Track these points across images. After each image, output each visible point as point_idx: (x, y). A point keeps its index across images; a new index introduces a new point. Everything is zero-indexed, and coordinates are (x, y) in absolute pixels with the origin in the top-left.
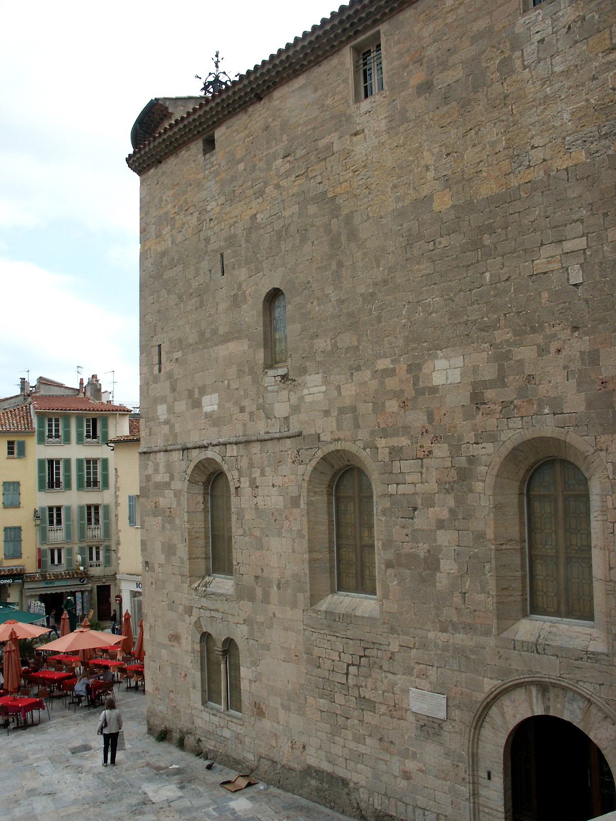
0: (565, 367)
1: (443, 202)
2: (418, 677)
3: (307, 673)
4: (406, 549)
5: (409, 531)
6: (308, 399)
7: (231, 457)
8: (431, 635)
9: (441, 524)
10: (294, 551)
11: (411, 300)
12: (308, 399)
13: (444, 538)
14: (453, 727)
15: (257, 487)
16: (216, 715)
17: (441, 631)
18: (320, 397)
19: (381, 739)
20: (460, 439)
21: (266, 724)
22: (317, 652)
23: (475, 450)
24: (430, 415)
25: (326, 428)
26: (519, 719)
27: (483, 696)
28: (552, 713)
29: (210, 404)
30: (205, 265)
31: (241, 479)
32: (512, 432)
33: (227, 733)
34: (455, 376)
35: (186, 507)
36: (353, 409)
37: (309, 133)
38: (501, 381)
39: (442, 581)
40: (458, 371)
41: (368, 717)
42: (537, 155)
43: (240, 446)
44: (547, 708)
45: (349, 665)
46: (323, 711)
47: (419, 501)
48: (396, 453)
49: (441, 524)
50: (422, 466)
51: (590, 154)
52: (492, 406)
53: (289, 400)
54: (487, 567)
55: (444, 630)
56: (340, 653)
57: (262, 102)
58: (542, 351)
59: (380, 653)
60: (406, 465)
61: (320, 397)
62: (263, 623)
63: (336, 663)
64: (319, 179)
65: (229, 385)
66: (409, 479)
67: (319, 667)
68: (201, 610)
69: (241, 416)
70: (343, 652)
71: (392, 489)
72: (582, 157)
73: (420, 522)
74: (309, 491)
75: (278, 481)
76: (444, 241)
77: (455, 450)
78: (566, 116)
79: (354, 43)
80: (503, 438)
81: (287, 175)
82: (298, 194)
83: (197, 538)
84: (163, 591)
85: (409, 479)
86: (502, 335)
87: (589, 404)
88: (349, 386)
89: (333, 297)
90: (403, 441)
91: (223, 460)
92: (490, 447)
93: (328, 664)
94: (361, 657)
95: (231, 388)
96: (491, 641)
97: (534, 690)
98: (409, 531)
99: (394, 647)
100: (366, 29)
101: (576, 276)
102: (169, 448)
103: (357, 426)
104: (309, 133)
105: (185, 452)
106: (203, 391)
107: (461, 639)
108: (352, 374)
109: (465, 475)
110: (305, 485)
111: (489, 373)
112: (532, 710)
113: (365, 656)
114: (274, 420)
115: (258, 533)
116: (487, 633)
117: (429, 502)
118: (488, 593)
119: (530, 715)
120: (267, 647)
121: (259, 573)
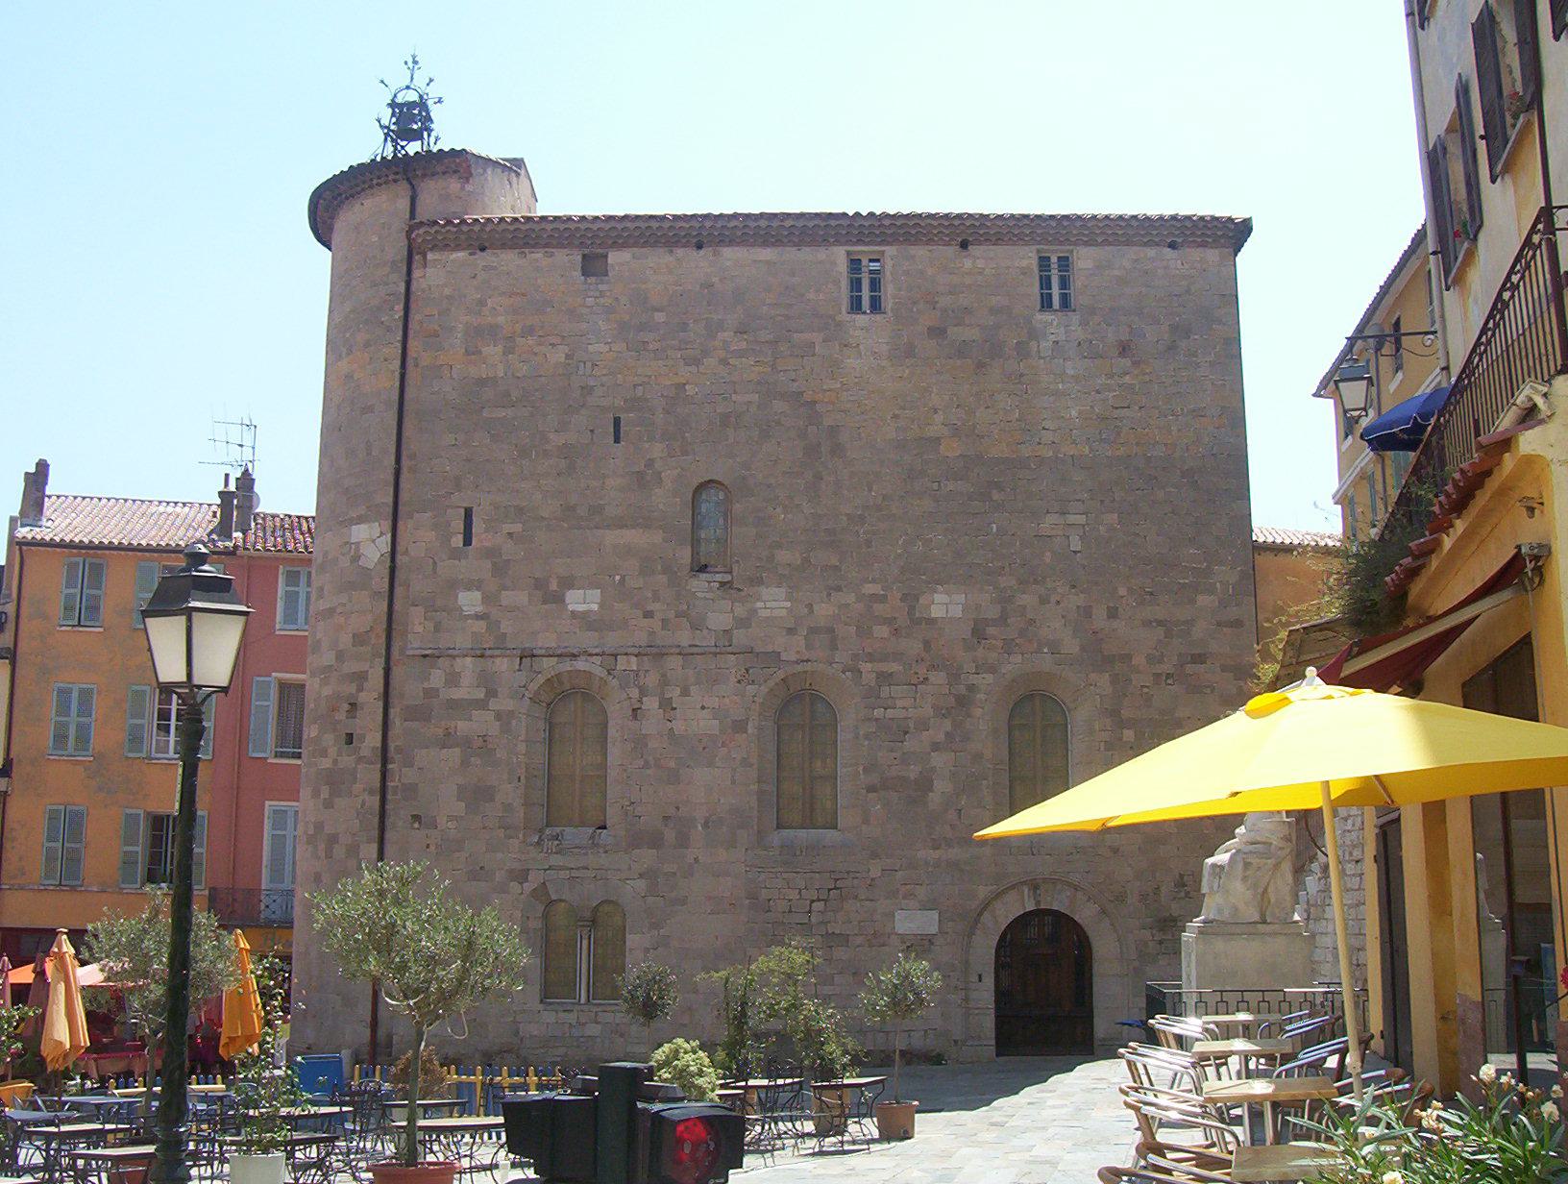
1: (951, 449)
2: (904, 898)
5: (898, 755)
6: (764, 613)
8: (921, 854)
9: (936, 747)
10: (733, 782)
11: (909, 532)
13: (938, 760)
14: (946, 940)
18: (784, 612)
22: (764, 894)
23: (974, 679)
24: (927, 644)
25: (792, 648)
29: (582, 601)
31: (644, 699)
32: (1010, 667)
33: (593, 1030)
34: (957, 611)
35: (524, 732)
36: (831, 630)
38: (1003, 620)
39: (935, 799)
41: (841, 953)
42: (1047, 437)
43: (646, 658)
44: (1038, 903)
47: (912, 725)
49: (936, 747)
50: (916, 692)
51: (1091, 450)
53: (732, 611)
55: (935, 848)
57: (702, 252)
58: (1044, 601)
61: (784, 612)
62: (675, 874)
64: (793, 375)
68: (548, 872)
71: (878, 713)
72: (1087, 450)
73: (910, 744)
75: (714, 702)
77: (954, 676)
78: (1074, 413)
80: (1003, 671)
81: (740, 354)
82: (759, 383)
84: (457, 854)
86: (1005, 581)
87: (1083, 649)
90: (894, 667)
91: (609, 674)
92: (989, 678)
94: (830, 890)
98: (898, 755)
99: (875, 871)
100: (880, 244)
101: (1076, 544)
102: (488, 653)
103: (834, 647)
106: (568, 583)
109: (963, 702)
111: (993, 612)
114: (705, 631)
115: (672, 764)
117: (923, 725)
120: (683, 901)
121: (672, 811)
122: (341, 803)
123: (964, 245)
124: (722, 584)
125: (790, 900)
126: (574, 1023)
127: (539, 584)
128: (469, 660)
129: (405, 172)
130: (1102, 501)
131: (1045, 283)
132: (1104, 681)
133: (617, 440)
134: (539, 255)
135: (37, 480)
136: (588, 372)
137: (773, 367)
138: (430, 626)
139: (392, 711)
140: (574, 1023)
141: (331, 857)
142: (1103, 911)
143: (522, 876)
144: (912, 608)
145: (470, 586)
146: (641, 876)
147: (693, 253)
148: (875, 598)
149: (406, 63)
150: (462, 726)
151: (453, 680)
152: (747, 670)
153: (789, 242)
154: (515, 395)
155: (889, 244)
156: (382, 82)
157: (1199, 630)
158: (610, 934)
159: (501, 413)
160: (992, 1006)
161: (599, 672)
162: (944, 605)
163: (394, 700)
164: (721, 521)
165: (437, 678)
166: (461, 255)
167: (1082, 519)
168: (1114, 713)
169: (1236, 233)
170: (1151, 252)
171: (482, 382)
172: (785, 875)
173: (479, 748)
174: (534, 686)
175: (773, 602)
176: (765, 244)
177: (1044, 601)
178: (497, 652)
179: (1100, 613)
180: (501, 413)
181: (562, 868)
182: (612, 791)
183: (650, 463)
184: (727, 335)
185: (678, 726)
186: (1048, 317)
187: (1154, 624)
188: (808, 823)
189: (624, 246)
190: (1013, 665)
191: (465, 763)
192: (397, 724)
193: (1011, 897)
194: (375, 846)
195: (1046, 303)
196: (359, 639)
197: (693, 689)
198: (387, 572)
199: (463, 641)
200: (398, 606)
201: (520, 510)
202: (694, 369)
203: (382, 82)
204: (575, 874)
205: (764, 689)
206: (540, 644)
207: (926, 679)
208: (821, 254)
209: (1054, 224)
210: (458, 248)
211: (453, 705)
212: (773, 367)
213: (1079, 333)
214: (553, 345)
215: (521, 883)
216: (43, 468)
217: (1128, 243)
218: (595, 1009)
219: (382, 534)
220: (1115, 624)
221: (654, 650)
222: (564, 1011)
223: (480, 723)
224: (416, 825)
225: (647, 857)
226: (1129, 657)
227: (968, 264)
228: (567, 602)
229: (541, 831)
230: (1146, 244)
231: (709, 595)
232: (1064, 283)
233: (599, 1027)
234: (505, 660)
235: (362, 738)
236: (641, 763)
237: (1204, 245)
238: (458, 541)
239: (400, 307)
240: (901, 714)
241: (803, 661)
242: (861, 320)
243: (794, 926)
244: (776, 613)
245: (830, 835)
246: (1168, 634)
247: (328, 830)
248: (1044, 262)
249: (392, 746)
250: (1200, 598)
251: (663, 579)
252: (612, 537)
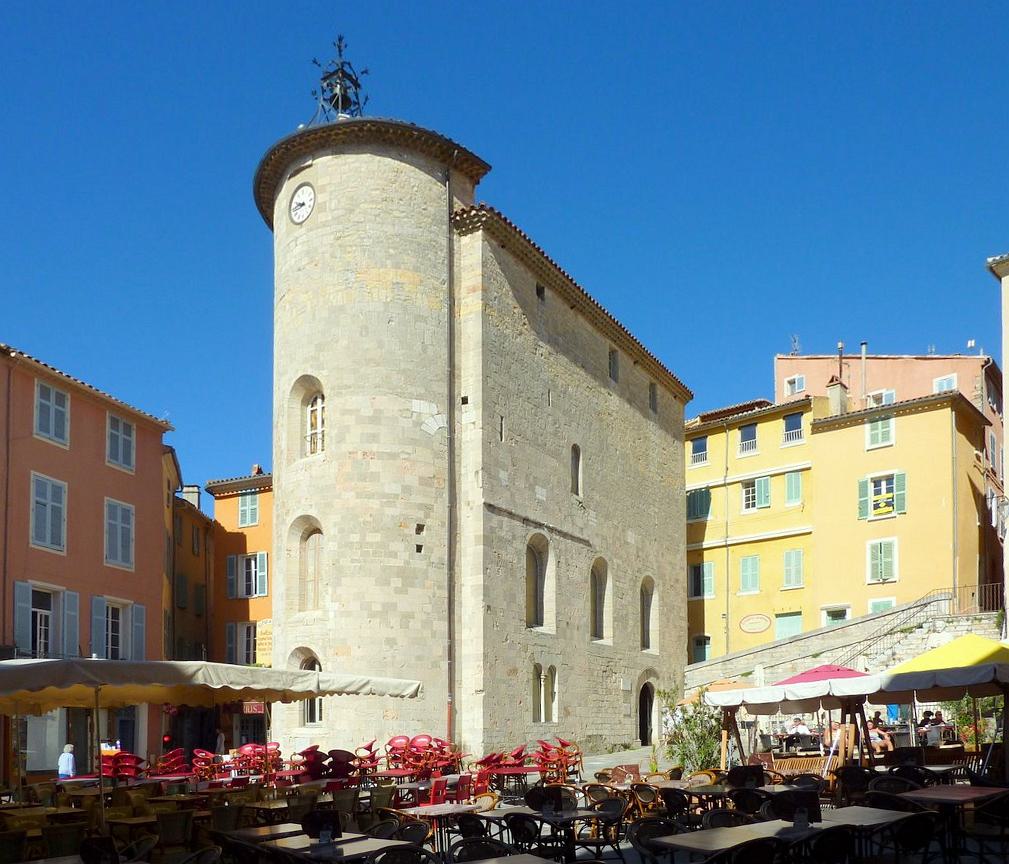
194: (446, 623)
196: (425, 482)
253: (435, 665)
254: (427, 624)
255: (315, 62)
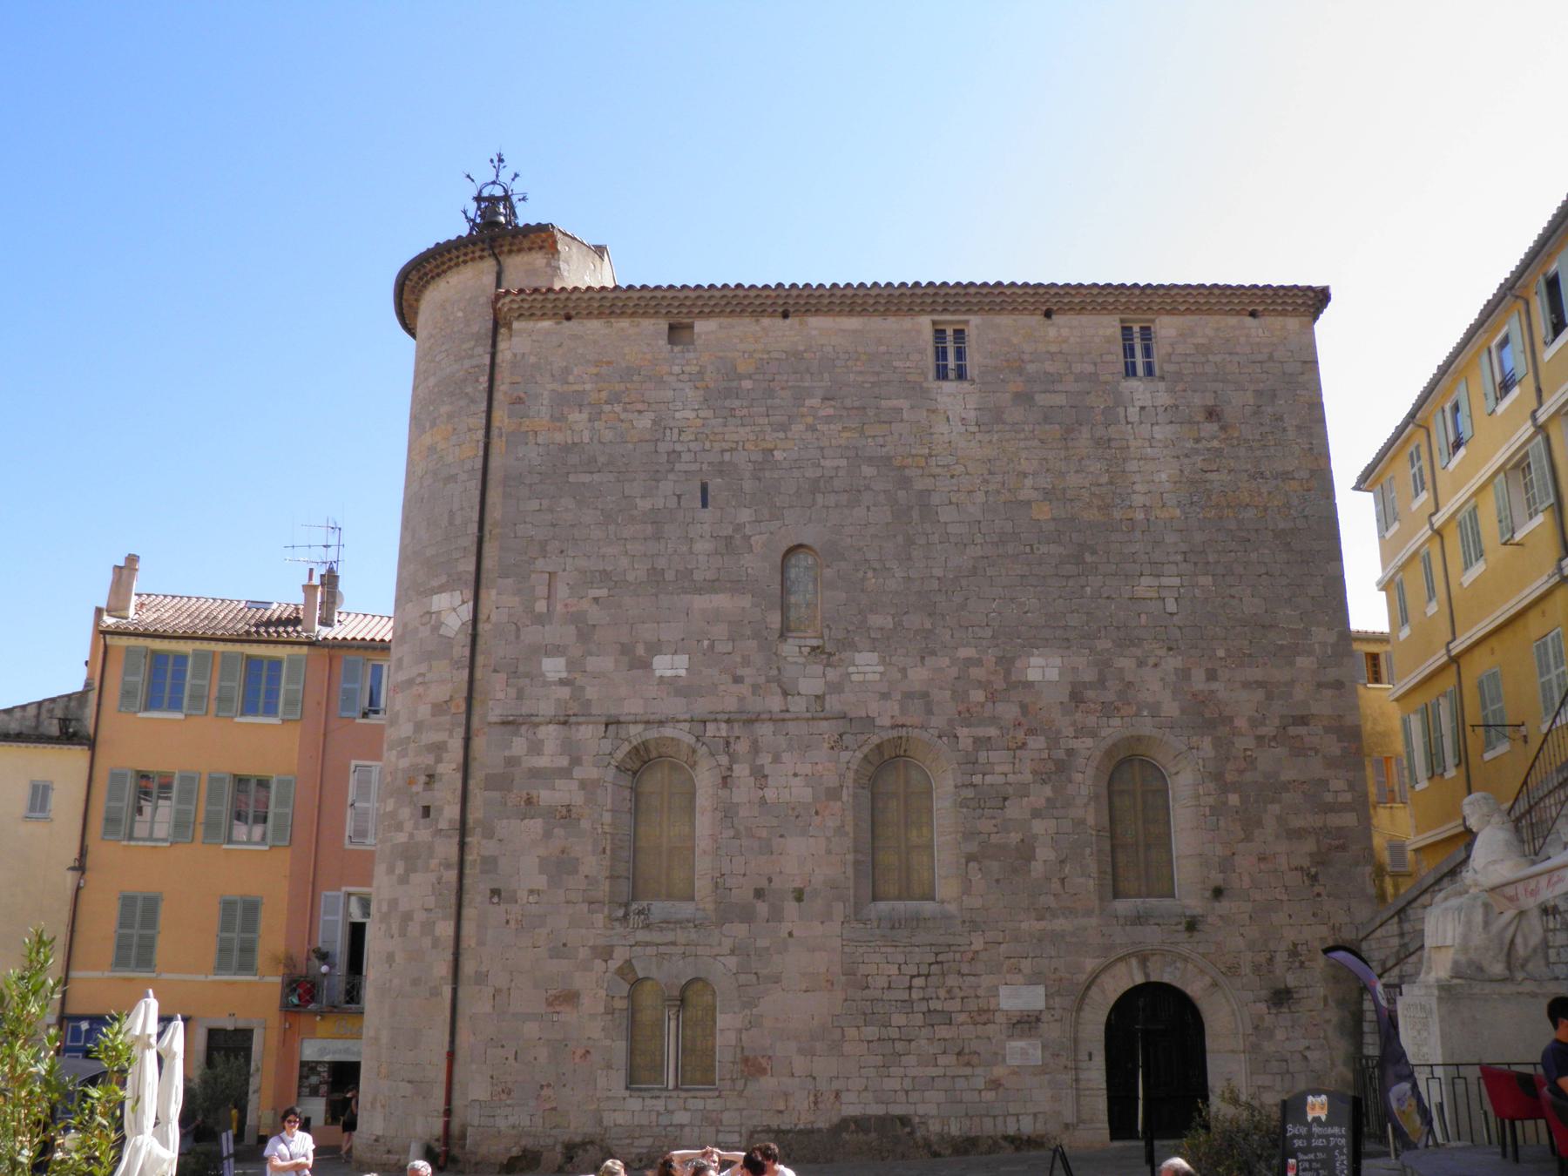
0: (1162, 679)
1: (1043, 512)
2: (1008, 972)
3: (846, 1000)
4: (994, 839)
7: (714, 737)
8: (1025, 926)
10: (829, 852)
12: (855, 678)
13: (1038, 827)
14: (1053, 1015)
15: (766, 777)
16: (659, 1097)
17: (1038, 920)
18: (877, 677)
19: (959, 1054)
20: (1059, 732)
21: (768, 1083)
22: (863, 969)
24: (1024, 708)
26: (1120, 992)
27: (1085, 977)
28: (1154, 979)
29: (667, 666)
30: (667, 487)
31: (734, 766)
32: (1110, 730)
33: (681, 1117)
34: (1053, 675)
37: (866, 385)
38: (1101, 683)
39: (1037, 868)
40: (1056, 671)
41: (943, 1032)
44: (1147, 975)
45: (912, 977)
46: (872, 1041)
48: (981, 743)
49: (1036, 814)
50: (1014, 757)
52: (1092, 706)
54: (1088, 851)
55: (1040, 918)
56: (900, 965)
57: (788, 321)
58: (1141, 664)
59: (958, 956)
60: (995, 756)
61: (877, 677)
63: (894, 978)
64: (880, 441)
65: (712, 646)
66: (998, 769)
67: (868, 987)
68: (634, 948)
69: (735, 688)
70: (905, 963)
73: (1013, 811)
74: (855, 781)
75: (806, 769)
76: (1044, 549)
77: (1054, 740)
78: (1164, 476)
79: (936, 317)
81: (828, 420)
82: (847, 448)
83: (621, 848)
85: (998, 769)
86: (1104, 644)
87: (1183, 711)
88: (919, 669)
89: (899, 574)
90: (993, 732)
91: (698, 740)
92: (1089, 742)
93: (882, 982)
94: (930, 964)
95: (716, 650)
96: (1094, 921)
97: (1134, 962)
99: (978, 944)
101: (1171, 606)
102: (573, 719)
103: (929, 712)
104: (866, 385)
105: (612, 728)
106: (656, 648)
107: (1060, 924)
108: (923, 658)
110: (851, 774)
111: (1089, 676)
112: (1133, 980)
113: (937, 963)
115: (764, 834)
116: (1088, 913)
117: (1023, 791)
118: (1090, 876)
119: (1131, 985)
120: (777, 980)
121: (764, 883)
122: (416, 878)
123: (1048, 314)
124: (814, 649)
125: (889, 976)
126: (662, 1109)
127: (626, 650)
128: (551, 727)
129: (492, 248)
130: (1195, 564)
131: (1129, 351)
132: (1207, 744)
133: (705, 505)
134: (624, 323)
135: (125, 572)
136: (675, 437)
137: (862, 432)
138: (512, 692)
139: (472, 783)
140: (662, 1109)
141: (405, 936)
142: (1215, 984)
143: (606, 953)
144: (1008, 672)
145: (556, 650)
146: (732, 952)
147: (779, 322)
148: (969, 662)
149: (492, 161)
150: (545, 796)
151: (536, 748)
152: (841, 736)
153: (875, 311)
154: (602, 459)
155: (976, 313)
156: (468, 176)
157: (1299, 694)
158: (700, 1013)
159: (586, 478)
160: (1104, 1085)
161: (689, 739)
162: (1042, 668)
163: (474, 766)
164: (811, 587)
165: (519, 746)
166: (546, 324)
167: (1176, 581)
168: (1218, 777)
169: (1316, 300)
170: (1233, 321)
171: (567, 448)
172: (883, 950)
173: (566, 816)
174: (620, 755)
175: (866, 665)
176: (851, 313)
177: (1141, 664)
178: (581, 719)
179: (1198, 676)
180: (586, 478)
181: (647, 944)
182: (703, 865)
183: (739, 528)
184: (814, 402)
185: (770, 794)
186: (1133, 383)
187: (1254, 686)
188: (905, 894)
189: (710, 314)
190: (1114, 729)
191: (548, 835)
192: (478, 797)
193: (1121, 969)
195: (1130, 371)
196: (439, 709)
197: (786, 757)
198: (468, 640)
199: (546, 708)
200: (478, 674)
201: (606, 575)
202: (781, 435)
203: (468, 176)
204: (662, 949)
205: (859, 755)
206: (626, 711)
207: (1024, 744)
208: (907, 323)
209: (1137, 292)
210: (543, 316)
211: (536, 774)
212: (862, 432)
213: (1164, 399)
214: (640, 412)
215: (606, 961)
216: (132, 560)
217: (1210, 312)
218: (683, 1094)
219: (463, 602)
220: (1214, 686)
221: (744, 717)
222: (652, 1098)
223: (563, 793)
224: (495, 900)
225: (740, 930)
226: (1231, 719)
227: (1052, 332)
228: (654, 667)
229: (627, 905)
230: (1227, 313)
231: (801, 660)
232: (1147, 352)
233: (689, 1114)
234: (591, 727)
235: (440, 810)
236: (731, 833)
237: (1284, 313)
238: (541, 606)
239: (484, 379)
240: (1000, 780)
241: (898, 726)
242: (949, 386)
243: (894, 1003)
244: (870, 677)
245: (928, 907)
246: (1269, 697)
247: (403, 906)
248: (1126, 331)
249: (471, 819)
250: (1299, 659)
251: (753, 644)
252: (700, 602)
253: (435, 993)
254: (428, 927)
255: (516, 175)
